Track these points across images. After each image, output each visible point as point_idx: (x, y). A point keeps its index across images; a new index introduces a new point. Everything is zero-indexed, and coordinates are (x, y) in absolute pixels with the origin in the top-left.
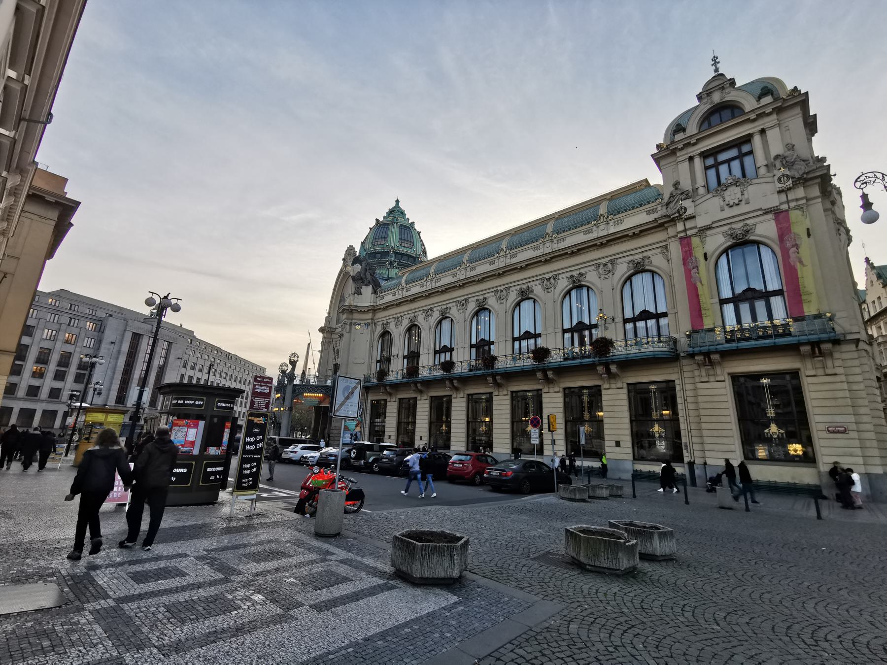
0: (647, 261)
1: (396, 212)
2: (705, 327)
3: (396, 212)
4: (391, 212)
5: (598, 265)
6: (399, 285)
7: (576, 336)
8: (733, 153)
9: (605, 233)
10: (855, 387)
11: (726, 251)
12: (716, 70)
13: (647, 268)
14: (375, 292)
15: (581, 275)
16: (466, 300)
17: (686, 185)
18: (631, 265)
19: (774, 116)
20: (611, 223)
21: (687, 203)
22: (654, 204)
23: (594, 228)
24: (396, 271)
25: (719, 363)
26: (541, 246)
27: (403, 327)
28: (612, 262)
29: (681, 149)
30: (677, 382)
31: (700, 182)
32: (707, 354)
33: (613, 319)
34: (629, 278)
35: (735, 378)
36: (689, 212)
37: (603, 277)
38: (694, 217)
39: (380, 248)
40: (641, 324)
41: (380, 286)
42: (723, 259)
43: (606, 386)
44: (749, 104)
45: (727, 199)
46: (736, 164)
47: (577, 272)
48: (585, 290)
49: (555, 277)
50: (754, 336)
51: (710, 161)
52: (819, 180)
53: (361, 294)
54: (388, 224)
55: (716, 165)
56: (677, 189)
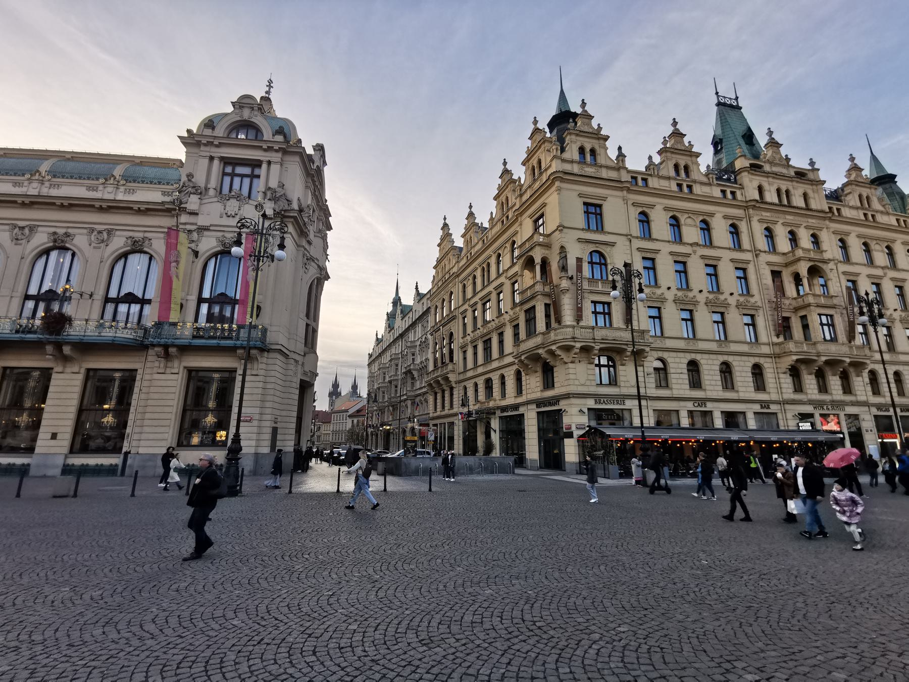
0: (147, 242)
2: (171, 321)
5: (92, 230)
7: (42, 306)
8: (247, 170)
9: (111, 197)
10: (269, 386)
11: (215, 255)
12: (268, 92)
13: (145, 249)
15: (67, 235)
17: (200, 179)
18: (129, 241)
19: (280, 155)
20: (122, 189)
21: (194, 199)
22: (171, 187)
23: (101, 188)
25: (177, 357)
26: (26, 183)
28: (109, 232)
29: (205, 145)
30: (139, 372)
31: (213, 183)
32: (166, 347)
33: (91, 296)
34: (125, 255)
35: (191, 373)
37: (93, 245)
38: (197, 214)
40: (123, 308)
42: (213, 260)
43: (60, 369)
44: (267, 134)
45: (228, 208)
46: (247, 181)
47: (64, 231)
48: (69, 255)
49: (32, 229)
50: (207, 335)
51: (229, 169)
52: (292, 220)
55: (233, 175)
56: (189, 180)
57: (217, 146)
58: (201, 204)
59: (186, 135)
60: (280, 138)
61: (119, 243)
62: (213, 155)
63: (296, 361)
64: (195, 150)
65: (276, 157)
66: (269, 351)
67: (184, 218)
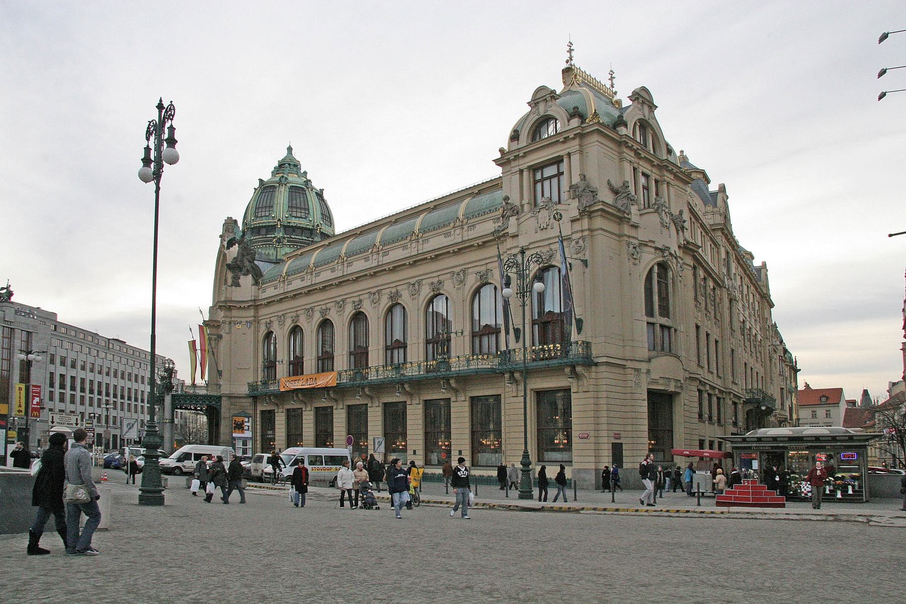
1: (288, 165)
3: (288, 165)
4: (281, 165)
5: (453, 273)
6: (287, 270)
8: (550, 171)
14: (256, 283)
15: (440, 282)
16: (343, 301)
17: (515, 200)
19: (577, 142)
24: (288, 250)
27: (286, 328)
29: (514, 160)
33: (462, 333)
34: (477, 291)
36: (511, 230)
39: (265, 221)
41: (261, 276)
49: (419, 283)
52: (599, 213)
53: (238, 285)
54: (274, 187)
55: (543, 180)
56: (507, 203)
57: (523, 157)
58: (519, 225)
59: (499, 156)
60: (575, 122)
61: (472, 281)
62: (521, 167)
63: (637, 370)
64: (508, 168)
65: (574, 145)
66: (596, 364)
67: (510, 243)
